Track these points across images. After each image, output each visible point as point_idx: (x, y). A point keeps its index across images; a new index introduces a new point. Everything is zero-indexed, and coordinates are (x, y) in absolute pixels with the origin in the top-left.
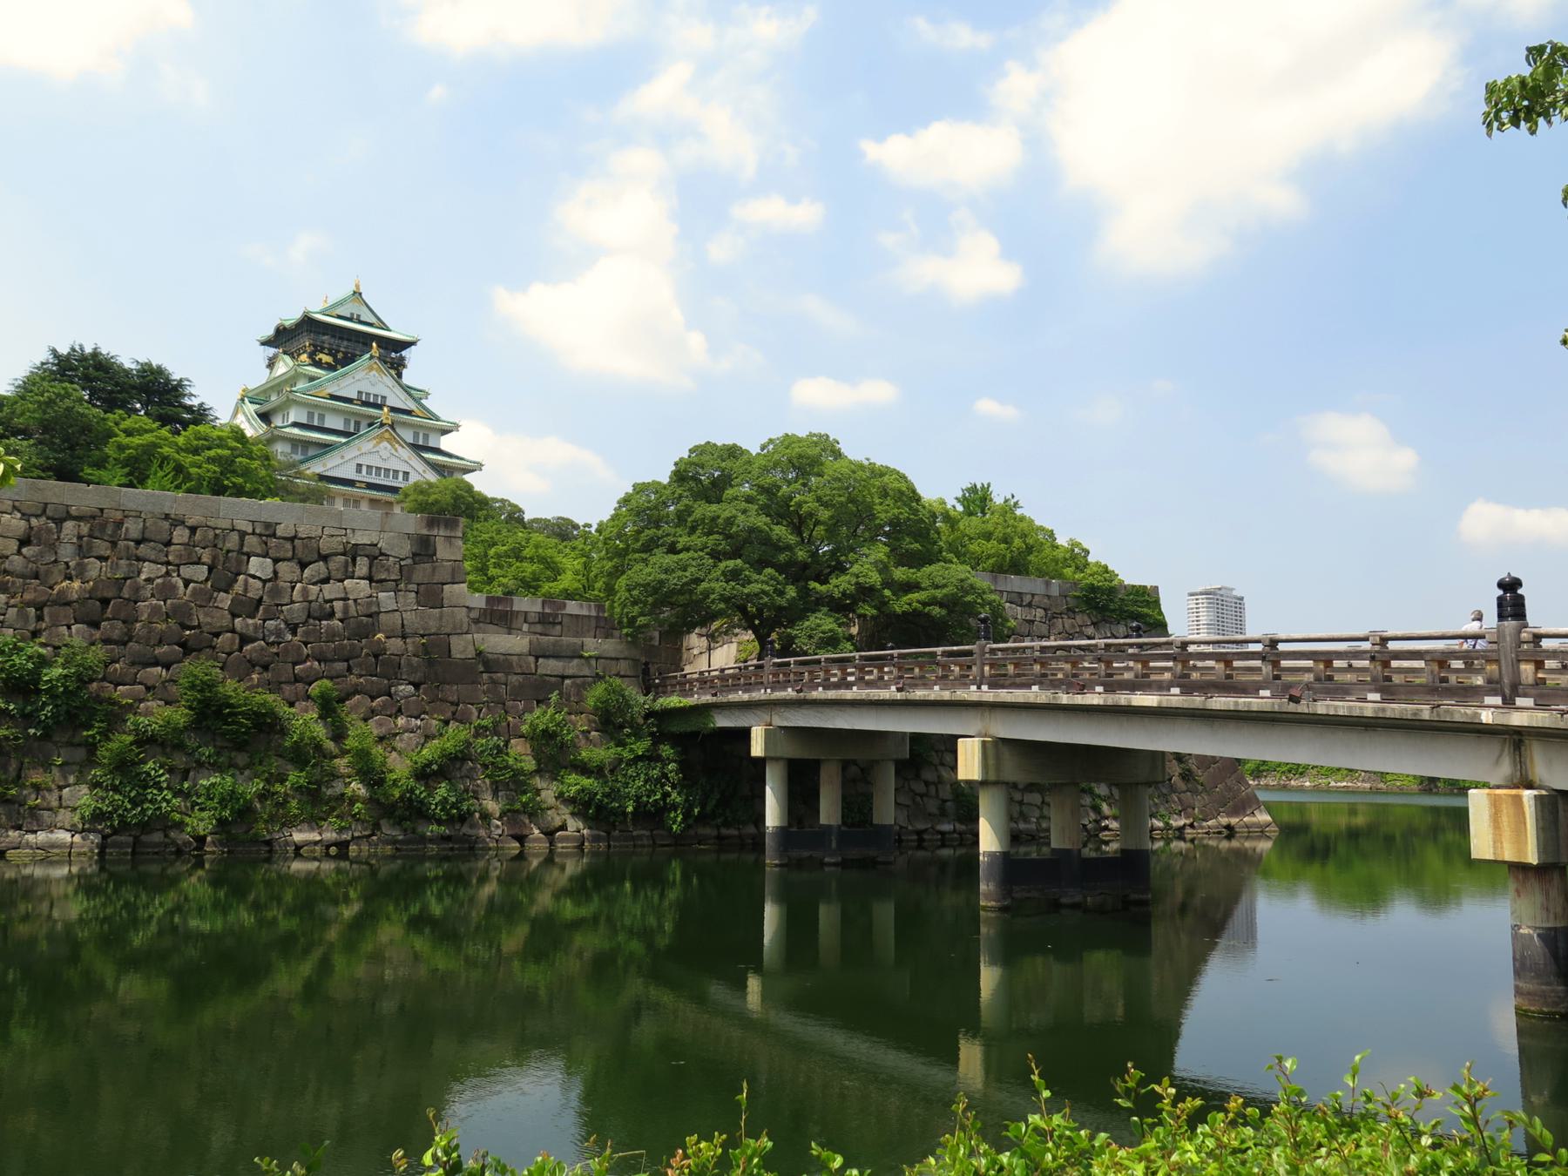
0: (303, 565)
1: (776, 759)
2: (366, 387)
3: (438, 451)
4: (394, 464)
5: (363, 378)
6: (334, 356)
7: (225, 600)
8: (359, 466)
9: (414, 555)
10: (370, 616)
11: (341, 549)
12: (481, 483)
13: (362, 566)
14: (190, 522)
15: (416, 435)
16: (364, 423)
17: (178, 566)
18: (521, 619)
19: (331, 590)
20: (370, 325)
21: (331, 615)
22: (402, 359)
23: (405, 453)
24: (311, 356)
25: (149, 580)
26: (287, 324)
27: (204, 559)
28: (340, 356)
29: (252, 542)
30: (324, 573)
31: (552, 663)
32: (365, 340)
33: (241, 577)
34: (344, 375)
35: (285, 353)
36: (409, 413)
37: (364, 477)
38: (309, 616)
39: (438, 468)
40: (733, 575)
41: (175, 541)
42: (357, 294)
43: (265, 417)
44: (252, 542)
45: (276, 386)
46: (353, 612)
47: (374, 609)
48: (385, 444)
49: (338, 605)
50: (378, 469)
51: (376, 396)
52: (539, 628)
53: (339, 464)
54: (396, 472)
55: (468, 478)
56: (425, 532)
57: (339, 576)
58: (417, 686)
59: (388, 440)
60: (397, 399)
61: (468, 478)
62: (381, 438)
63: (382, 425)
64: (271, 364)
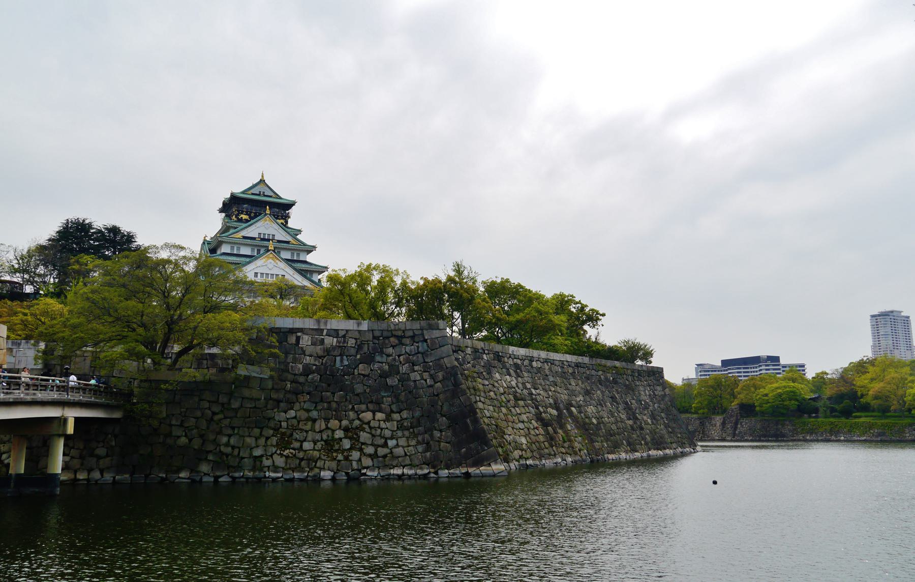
3: (305, 262)
6: (249, 215)
20: (271, 197)
28: (252, 215)
36: (288, 242)
42: (262, 181)
60: (281, 235)
62: (268, 258)
63: (268, 251)
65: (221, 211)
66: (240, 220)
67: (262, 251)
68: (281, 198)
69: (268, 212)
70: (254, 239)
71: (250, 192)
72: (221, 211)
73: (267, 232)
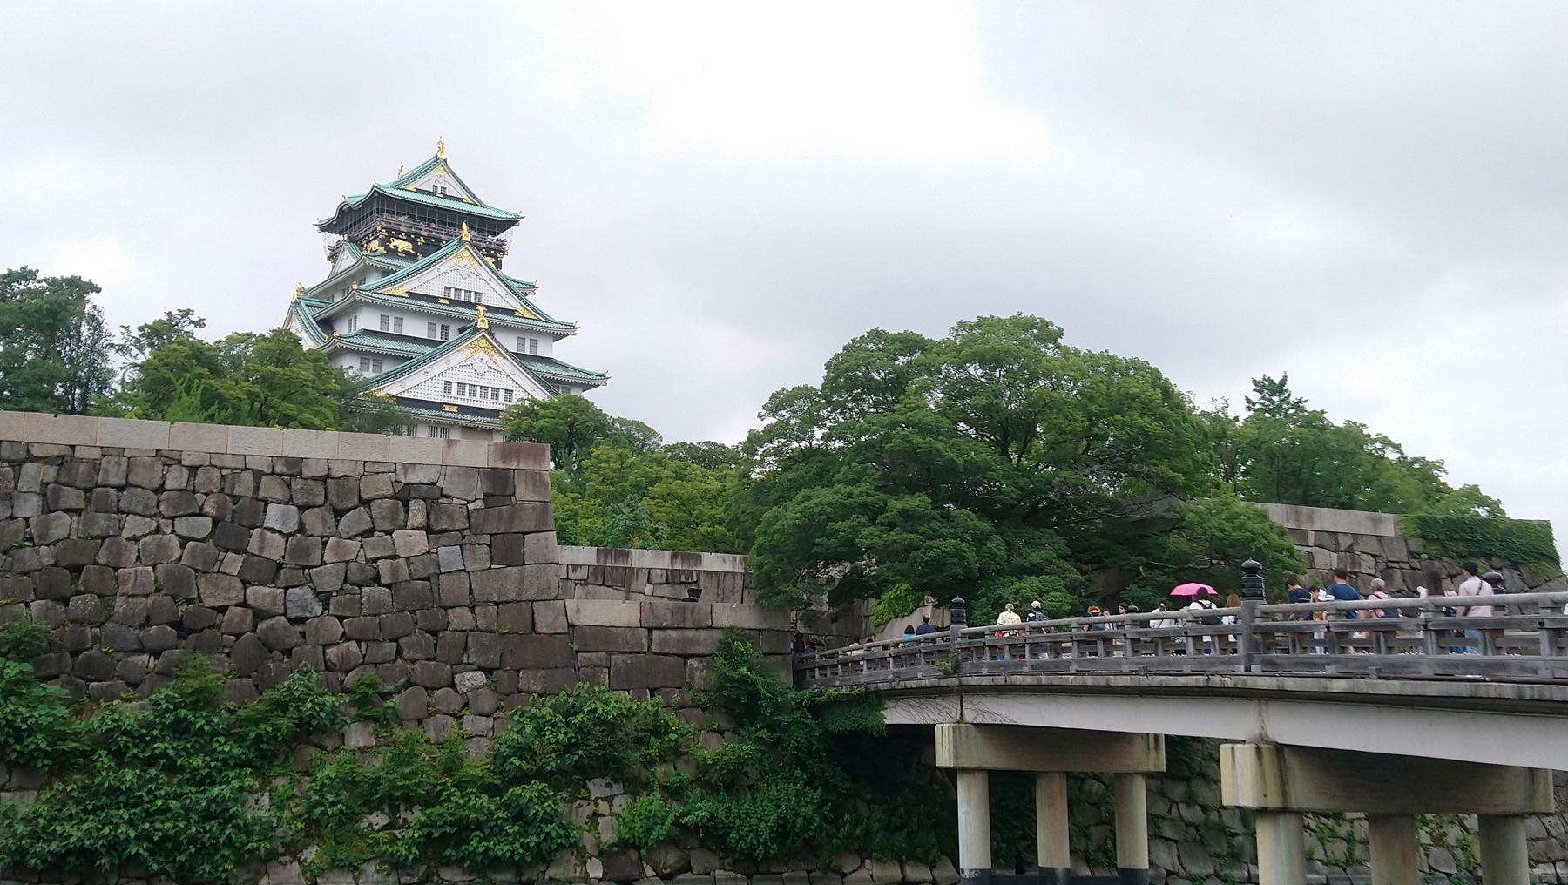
2: (454, 281)
4: (492, 380)
5: (455, 272)
8: (448, 383)
12: (600, 399)
20: (460, 200)
22: (503, 243)
23: (508, 366)
26: (352, 202)
28: (421, 241)
32: (451, 219)
35: (351, 240)
36: (511, 312)
37: (455, 398)
39: (549, 383)
43: (326, 324)
45: (339, 284)
48: (482, 354)
53: (422, 385)
54: (495, 390)
55: (588, 395)
59: (484, 349)
60: (496, 296)
61: (588, 395)
62: (477, 346)
63: (477, 330)
64: (334, 256)
66: (393, 253)
70: (435, 299)
73: (464, 286)
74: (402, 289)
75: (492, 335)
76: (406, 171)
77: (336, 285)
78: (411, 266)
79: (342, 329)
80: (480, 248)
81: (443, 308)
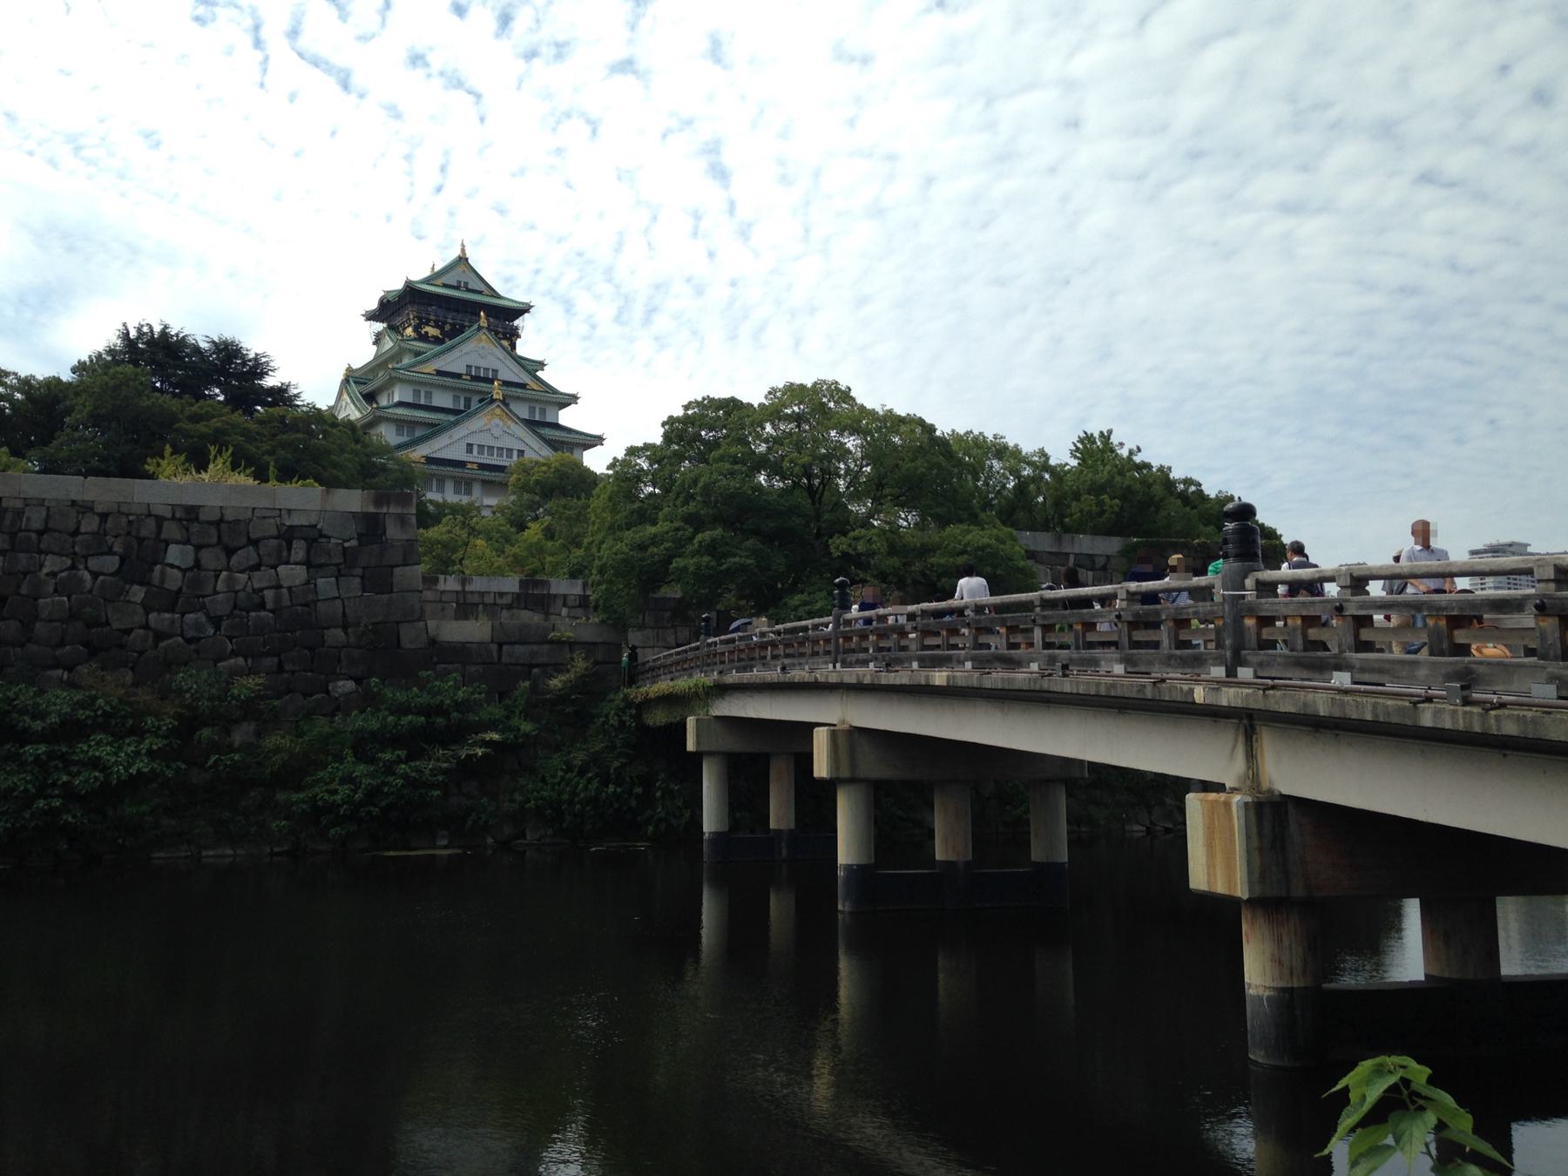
0: (230, 552)
1: (711, 754)
3: (557, 426)
6: (441, 328)
7: (138, 593)
9: (360, 536)
10: (307, 605)
11: (274, 532)
13: (299, 550)
14: (99, 509)
15: (532, 410)
16: (475, 399)
17: (86, 558)
18: (560, 602)
19: (261, 579)
20: (480, 293)
21: (262, 606)
23: (521, 431)
24: (416, 329)
25: (53, 574)
27: (116, 549)
28: (447, 327)
29: (171, 530)
30: (254, 560)
31: (520, 649)
32: (472, 309)
33: (158, 568)
34: (453, 347)
36: (523, 386)
37: (475, 457)
38: (235, 607)
39: (554, 445)
40: (712, 549)
41: (83, 529)
42: (462, 260)
43: (370, 397)
44: (171, 530)
46: (286, 601)
47: (311, 597)
48: (497, 421)
49: (269, 595)
50: (491, 448)
51: (486, 370)
52: (579, 612)
54: (510, 451)
56: (372, 509)
57: (272, 561)
58: (358, 681)
59: (500, 417)
63: (493, 401)
65: (371, 317)
66: (424, 338)
67: (474, 405)
68: (499, 297)
69: (483, 322)
70: (458, 376)
71: (439, 282)
72: (371, 317)
73: (483, 364)
74: (430, 368)
75: (507, 405)
76: (437, 269)
77: (379, 366)
78: (438, 348)
79: (383, 401)
80: (497, 333)
81: (466, 383)
